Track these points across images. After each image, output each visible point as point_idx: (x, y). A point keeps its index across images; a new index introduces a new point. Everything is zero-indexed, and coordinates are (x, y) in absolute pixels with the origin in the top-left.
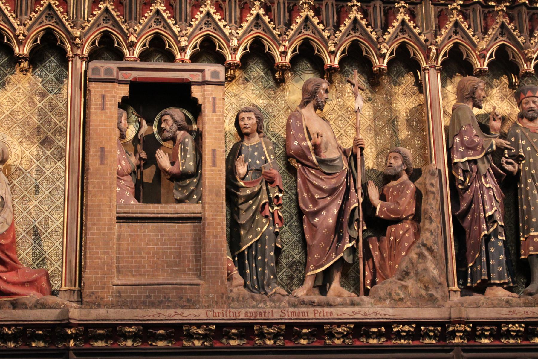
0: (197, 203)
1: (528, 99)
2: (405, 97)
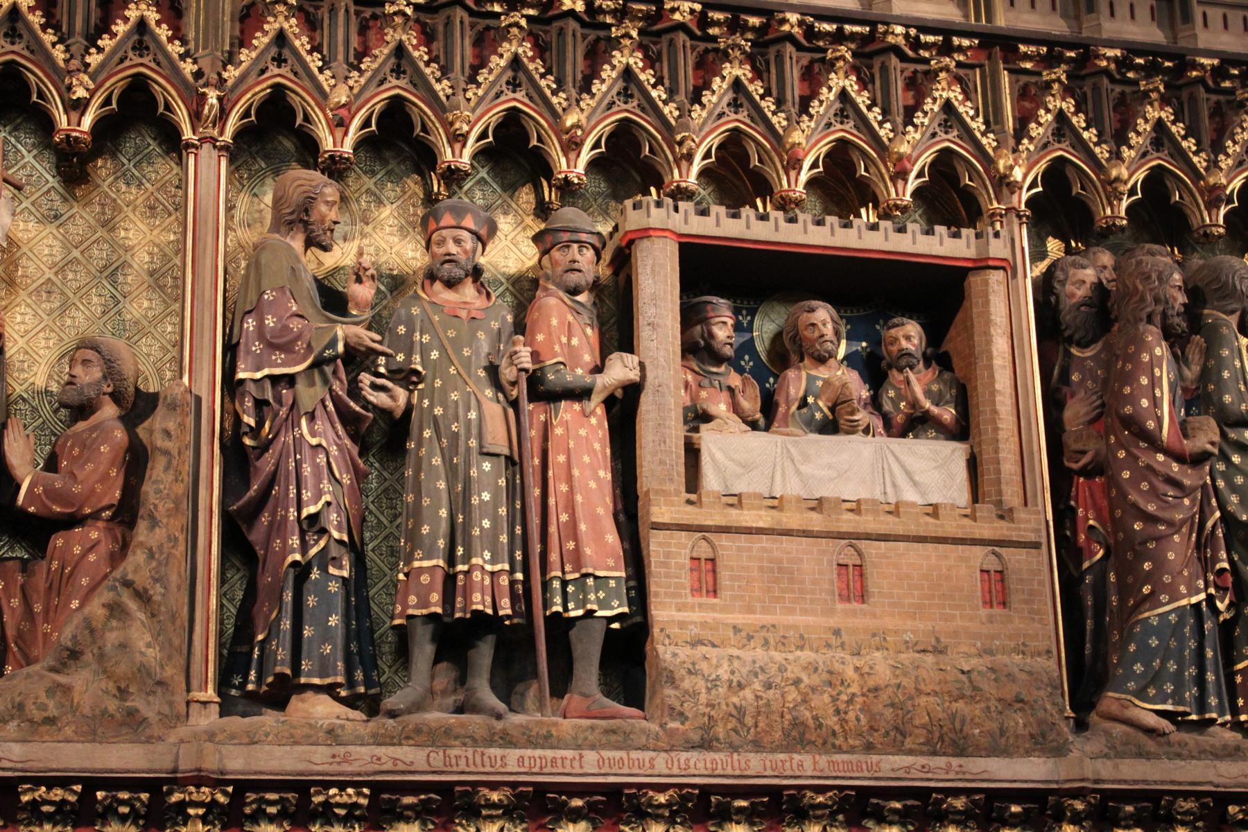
1: (444, 232)
2: (153, 216)
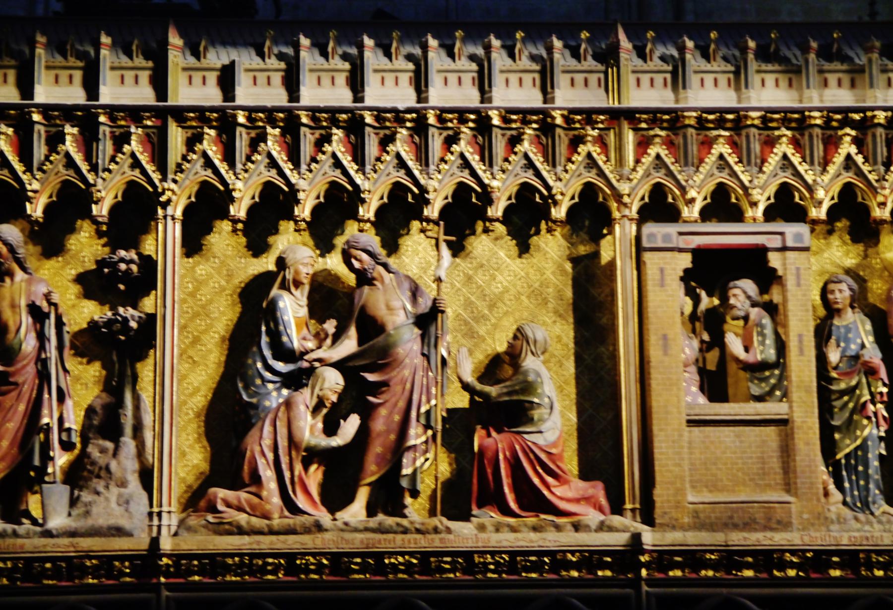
0: (781, 401)
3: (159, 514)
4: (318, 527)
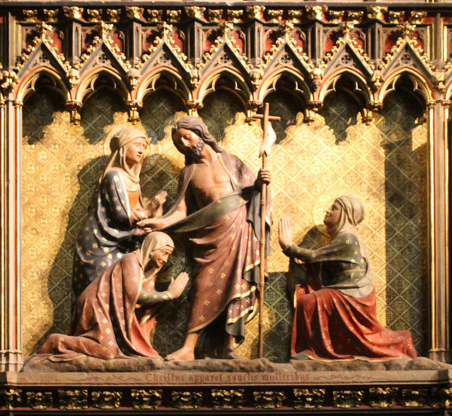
3: (7, 355)
4: (151, 366)
